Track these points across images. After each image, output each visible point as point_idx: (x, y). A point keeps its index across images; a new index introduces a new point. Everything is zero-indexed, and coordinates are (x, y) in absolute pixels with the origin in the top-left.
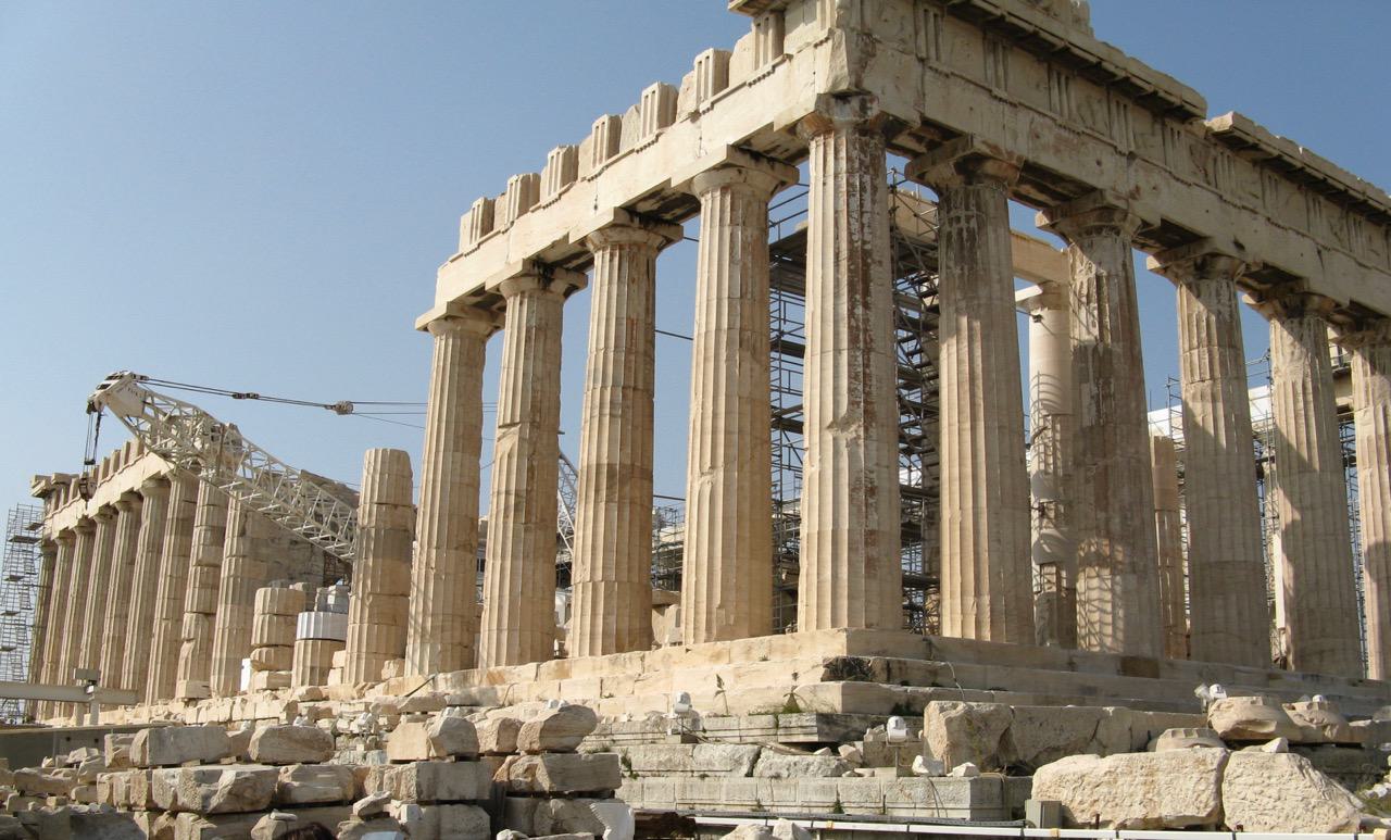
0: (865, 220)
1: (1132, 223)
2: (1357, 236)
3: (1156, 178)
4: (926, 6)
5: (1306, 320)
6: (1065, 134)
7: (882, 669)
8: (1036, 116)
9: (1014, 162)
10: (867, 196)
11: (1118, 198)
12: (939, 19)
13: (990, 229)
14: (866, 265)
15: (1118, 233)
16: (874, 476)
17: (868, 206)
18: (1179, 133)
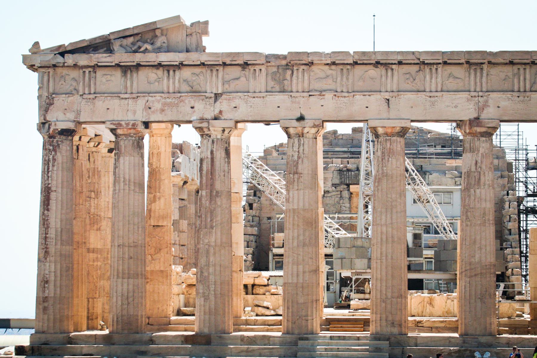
0: (50, 175)
1: (214, 131)
2: (431, 78)
3: (237, 102)
4: (84, 70)
5: (380, 140)
6: (170, 100)
7: (30, 350)
8: (150, 98)
9: (130, 127)
10: (51, 165)
11: (201, 123)
12: (92, 73)
13: (121, 159)
14: (49, 193)
15: (210, 136)
16: (48, 276)
17: (50, 169)
18: (261, 70)
